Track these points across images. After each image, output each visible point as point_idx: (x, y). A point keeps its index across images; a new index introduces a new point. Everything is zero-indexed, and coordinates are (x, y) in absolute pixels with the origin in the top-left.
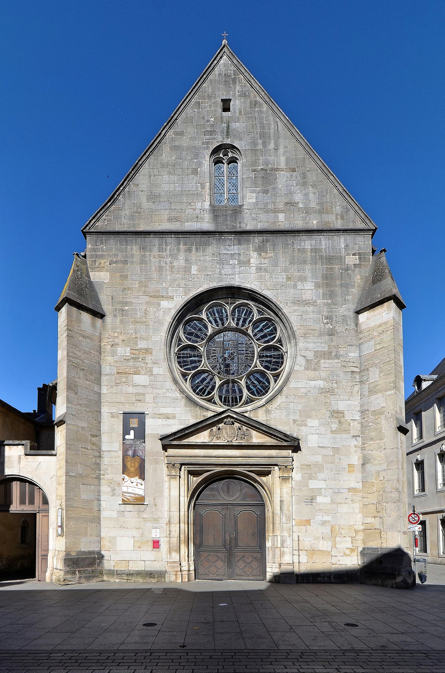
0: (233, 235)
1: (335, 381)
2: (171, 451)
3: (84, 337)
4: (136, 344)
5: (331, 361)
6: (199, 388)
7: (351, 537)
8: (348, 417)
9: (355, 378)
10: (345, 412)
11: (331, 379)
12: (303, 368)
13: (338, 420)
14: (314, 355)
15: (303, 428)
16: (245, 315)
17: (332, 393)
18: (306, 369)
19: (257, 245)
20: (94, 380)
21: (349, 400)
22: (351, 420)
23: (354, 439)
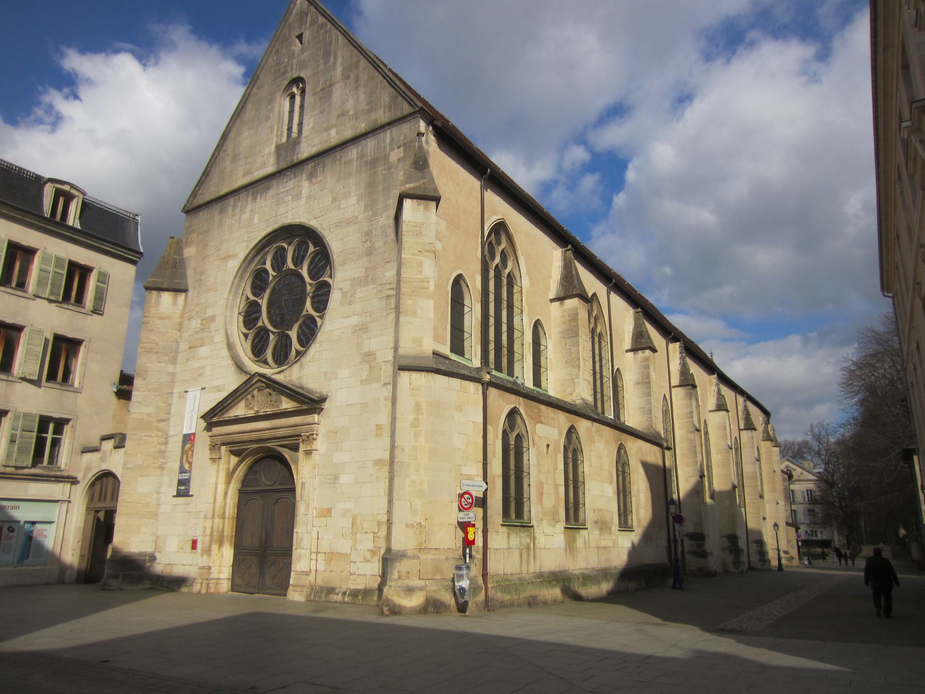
0: (290, 170)
1: (369, 314)
2: (216, 430)
3: (162, 318)
4: (205, 313)
5: (367, 288)
6: (258, 348)
7: (373, 533)
8: (380, 358)
9: (390, 304)
10: (378, 353)
11: (365, 311)
12: (338, 304)
13: (369, 365)
14: (351, 285)
15: (334, 382)
16: (303, 252)
17: (365, 330)
18: (341, 304)
19: (309, 172)
20: (169, 360)
21: (382, 335)
22: (384, 362)
23: (385, 387)
